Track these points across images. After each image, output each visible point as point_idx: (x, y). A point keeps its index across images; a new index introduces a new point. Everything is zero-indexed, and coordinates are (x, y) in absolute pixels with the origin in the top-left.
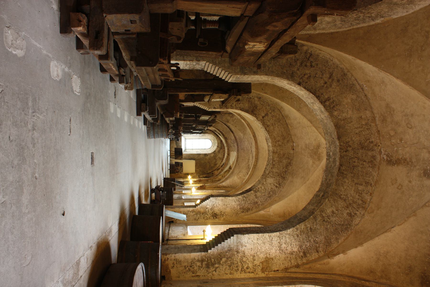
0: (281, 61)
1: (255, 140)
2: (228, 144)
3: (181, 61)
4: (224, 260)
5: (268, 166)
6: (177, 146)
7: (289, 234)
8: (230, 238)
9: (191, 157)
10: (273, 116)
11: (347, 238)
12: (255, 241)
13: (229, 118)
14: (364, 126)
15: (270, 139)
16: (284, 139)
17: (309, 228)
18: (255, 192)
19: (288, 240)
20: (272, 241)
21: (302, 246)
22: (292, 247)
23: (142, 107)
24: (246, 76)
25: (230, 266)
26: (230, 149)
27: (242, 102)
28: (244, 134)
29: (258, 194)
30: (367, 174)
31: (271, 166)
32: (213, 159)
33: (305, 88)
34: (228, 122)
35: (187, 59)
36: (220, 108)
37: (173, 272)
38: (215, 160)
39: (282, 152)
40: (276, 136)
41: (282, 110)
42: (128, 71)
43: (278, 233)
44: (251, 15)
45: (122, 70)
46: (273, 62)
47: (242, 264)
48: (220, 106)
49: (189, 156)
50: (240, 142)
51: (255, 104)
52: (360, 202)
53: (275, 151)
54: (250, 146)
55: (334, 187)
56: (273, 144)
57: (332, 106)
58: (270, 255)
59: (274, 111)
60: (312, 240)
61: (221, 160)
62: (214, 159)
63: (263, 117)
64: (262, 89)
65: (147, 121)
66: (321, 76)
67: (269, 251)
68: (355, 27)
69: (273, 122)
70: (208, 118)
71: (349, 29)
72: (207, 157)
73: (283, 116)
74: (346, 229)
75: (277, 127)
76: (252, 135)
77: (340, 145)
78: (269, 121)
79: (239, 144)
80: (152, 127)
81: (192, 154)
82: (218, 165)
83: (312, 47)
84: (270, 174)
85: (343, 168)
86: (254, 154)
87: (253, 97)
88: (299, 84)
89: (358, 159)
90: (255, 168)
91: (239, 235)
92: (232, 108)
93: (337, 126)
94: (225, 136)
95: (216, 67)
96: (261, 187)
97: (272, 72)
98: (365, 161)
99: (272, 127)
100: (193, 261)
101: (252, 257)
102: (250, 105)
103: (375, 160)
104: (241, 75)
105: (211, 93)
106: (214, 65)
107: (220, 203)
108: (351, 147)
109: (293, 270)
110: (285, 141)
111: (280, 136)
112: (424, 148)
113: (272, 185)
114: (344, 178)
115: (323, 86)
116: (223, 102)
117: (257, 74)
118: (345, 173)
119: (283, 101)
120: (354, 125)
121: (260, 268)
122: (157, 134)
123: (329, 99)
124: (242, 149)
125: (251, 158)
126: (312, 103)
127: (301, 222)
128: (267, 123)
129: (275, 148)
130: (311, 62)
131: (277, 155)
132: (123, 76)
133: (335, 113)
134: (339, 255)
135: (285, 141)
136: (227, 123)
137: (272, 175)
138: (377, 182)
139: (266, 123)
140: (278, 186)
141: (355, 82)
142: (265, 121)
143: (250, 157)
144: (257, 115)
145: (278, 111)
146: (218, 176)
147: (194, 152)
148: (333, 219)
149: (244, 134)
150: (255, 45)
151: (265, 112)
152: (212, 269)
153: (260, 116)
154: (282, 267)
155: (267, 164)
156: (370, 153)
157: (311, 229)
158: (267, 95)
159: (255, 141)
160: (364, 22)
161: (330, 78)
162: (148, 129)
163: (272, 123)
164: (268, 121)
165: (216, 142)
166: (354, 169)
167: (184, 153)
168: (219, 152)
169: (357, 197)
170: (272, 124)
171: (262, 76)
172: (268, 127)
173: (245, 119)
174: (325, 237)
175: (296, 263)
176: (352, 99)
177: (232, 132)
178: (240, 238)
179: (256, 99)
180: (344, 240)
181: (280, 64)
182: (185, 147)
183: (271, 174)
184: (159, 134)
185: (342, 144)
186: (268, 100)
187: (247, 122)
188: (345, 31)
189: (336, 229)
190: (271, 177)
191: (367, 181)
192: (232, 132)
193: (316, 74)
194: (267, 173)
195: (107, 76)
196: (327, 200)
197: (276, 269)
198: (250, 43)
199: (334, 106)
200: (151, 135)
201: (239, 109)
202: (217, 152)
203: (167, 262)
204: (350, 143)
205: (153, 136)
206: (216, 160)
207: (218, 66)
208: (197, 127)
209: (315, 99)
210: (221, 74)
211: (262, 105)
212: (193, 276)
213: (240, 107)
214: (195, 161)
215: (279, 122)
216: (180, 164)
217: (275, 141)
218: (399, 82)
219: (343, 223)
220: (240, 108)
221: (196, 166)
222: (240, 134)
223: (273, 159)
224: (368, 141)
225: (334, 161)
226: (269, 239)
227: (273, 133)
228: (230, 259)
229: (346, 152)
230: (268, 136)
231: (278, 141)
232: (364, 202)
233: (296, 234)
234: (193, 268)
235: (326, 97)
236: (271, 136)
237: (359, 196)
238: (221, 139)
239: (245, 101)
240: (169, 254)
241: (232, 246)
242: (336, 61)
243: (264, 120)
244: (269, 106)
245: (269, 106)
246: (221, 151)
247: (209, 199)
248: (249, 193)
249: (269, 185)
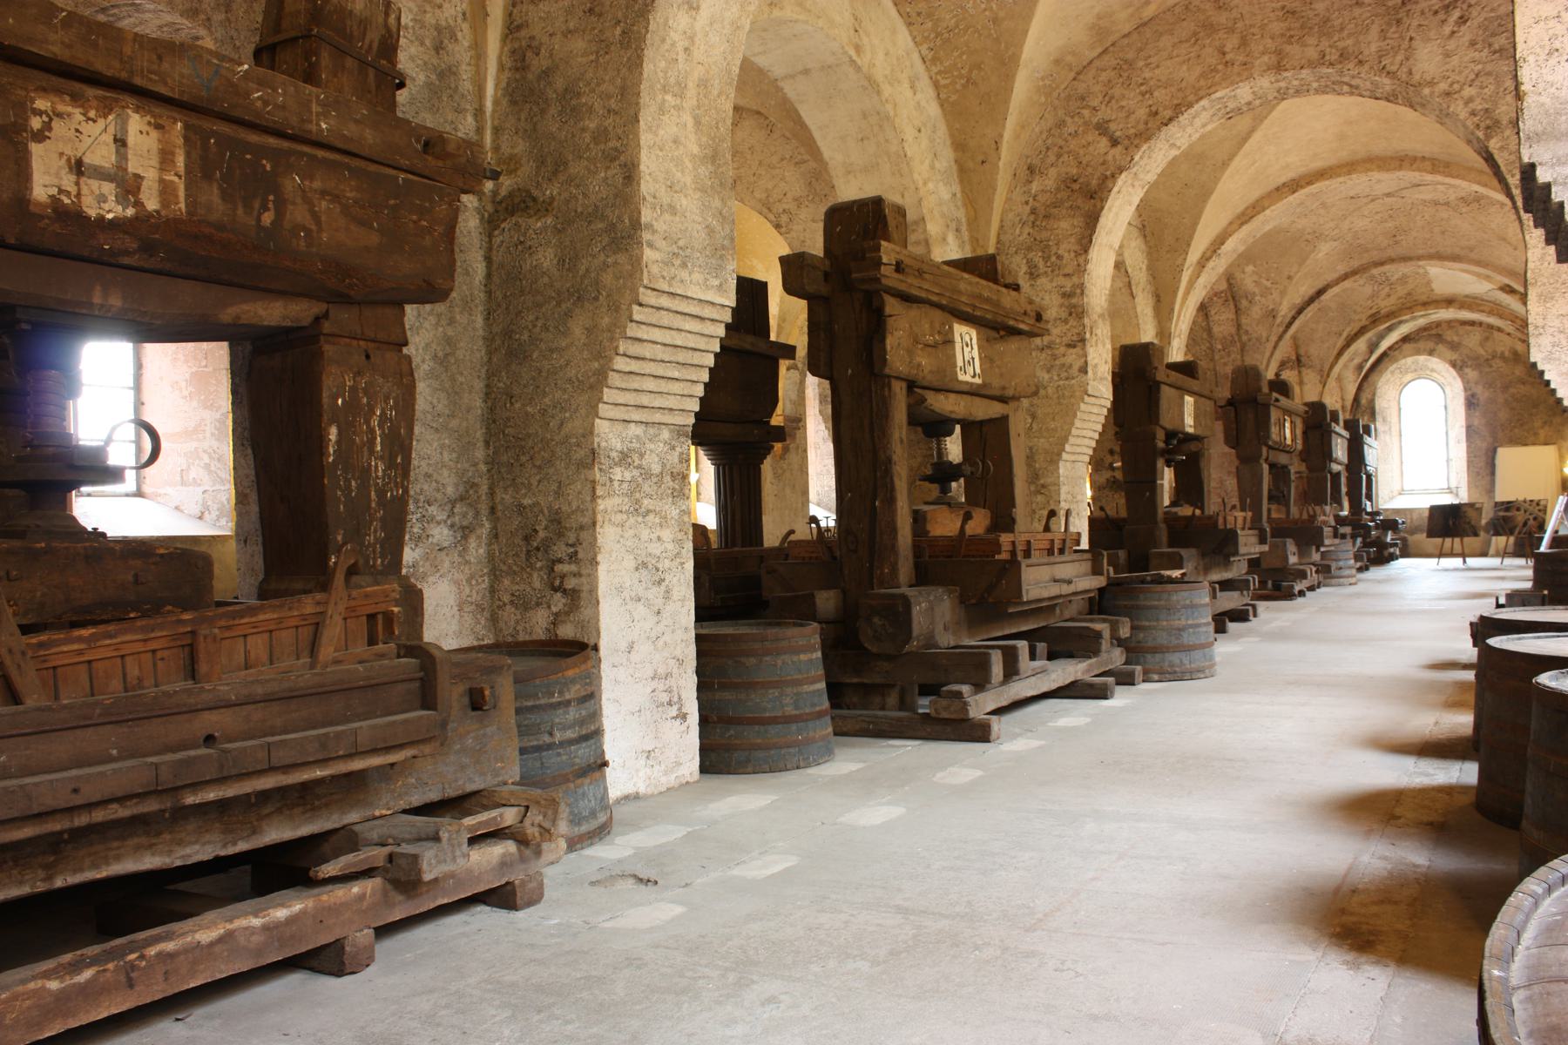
0: (579, 60)
1: (1309, 183)
2: (1401, 310)
3: (595, 539)
5: (1357, 87)
6: (1422, 531)
8: (1548, 186)
9: (1484, 466)
10: (1108, 99)
13: (1256, 312)
15: (1218, 95)
16: (1210, 28)
23: (945, 715)
26: (1424, 298)
27: (1054, 249)
28: (1318, 236)
31: (1351, 66)
32: (1488, 370)
34: (1272, 314)
35: (587, 510)
36: (1084, 345)
38: (1493, 363)
39: (1277, 27)
40: (1198, 70)
41: (1069, 58)
46: (584, 101)
48: (1075, 347)
49: (1478, 474)
50: (1366, 255)
51: (1058, 190)
53: (1274, 58)
54: (1366, 204)
56: (1239, 74)
59: (1083, 99)
61: (1496, 333)
62: (1491, 366)
63: (1115, 142)
64: (983, 162)
65: (1091, 686)
69: (1132, 95)
70: (1189, 400)
72: (1483, 394)
73: (1105, 51)
75: (1156, 71)
76: (1291, 198)
78: (1130, 113)
79: (1375, 256)
80: (1149, 656)
81: (1470, 463)
84: (1394, 68)
86: (1384, 181)
87: (1027, 203)
90: (1447, 165)
92: (1078, 291)
94: (1364, 323)
95: (614, 370)
97: (622, 95)
99: (1156, 94)
102: (1064, 211)
104: (640, 243)
105: (899, 389)
106: (606, 378)
110: (1222, 18)
111: (1197, 47)
117: (633, 164)
122: (1185, 635)
124: (1396, 242)
125: (1426, 194)
128: (1138, 122)
129: (1257, 63)
131: (1294, 50)
135: (1222, 18)
136: (1279, 320)
137: (1399, 58)
139: (1141, 127)
142: (1132, 131)
143: (1421, 196)
144: (1108, 173)
145: (1081, 77)
147: (1460, 452)
149: (1318, 236)
151: (1090, 139)
153: (1110, 157)
155: (1351, 94)
158: (1007, 135)
159: (1317, 180)
162: (1156, 677)
163: (1140, 98)
164: (1133, 116)
165: (1409, 360)
167: (1463, 497)
168: (1454, 347)
170: (1143, 94)
172: (1156, 113)
173: (1217, 237)
177: (1320, 293)
178: (1547, 113)
179: (1035, 187)
181: (592, 61)
182: (1442, 491)
183: (1392, 62)
184: (1183, 622)
186: (1037, 130)
187: (1235, 226)
190: (1407, 59)
192: (1320, 293)
194: (1387, 81)
200: (1186, 661)
201: (1083, 257)
202: (1455, 356)
205: (1197, 654)
206: (1494, 357)
207: (611, 360)
208: (1286, 445)
210: (679, 343)
211: (1059, 156)
213: (1073, 254)
214: (1501, 446)
215: (1130, 64)
216: (1502, 514)
217: (1220, 67)
220: (1077, 254)
221: (1526, 445)
222: (1325, 259)
223: (1312, 65)
227: (1183, 85)
230: (1204, 109)
231: (1224, 54)
236: (1202, 93)
238: (1397, 343)
239: (1045, 235)
243: (1128, 137)
244: (1061, 124)
246: (1449, 339)
247: (1540, 367)
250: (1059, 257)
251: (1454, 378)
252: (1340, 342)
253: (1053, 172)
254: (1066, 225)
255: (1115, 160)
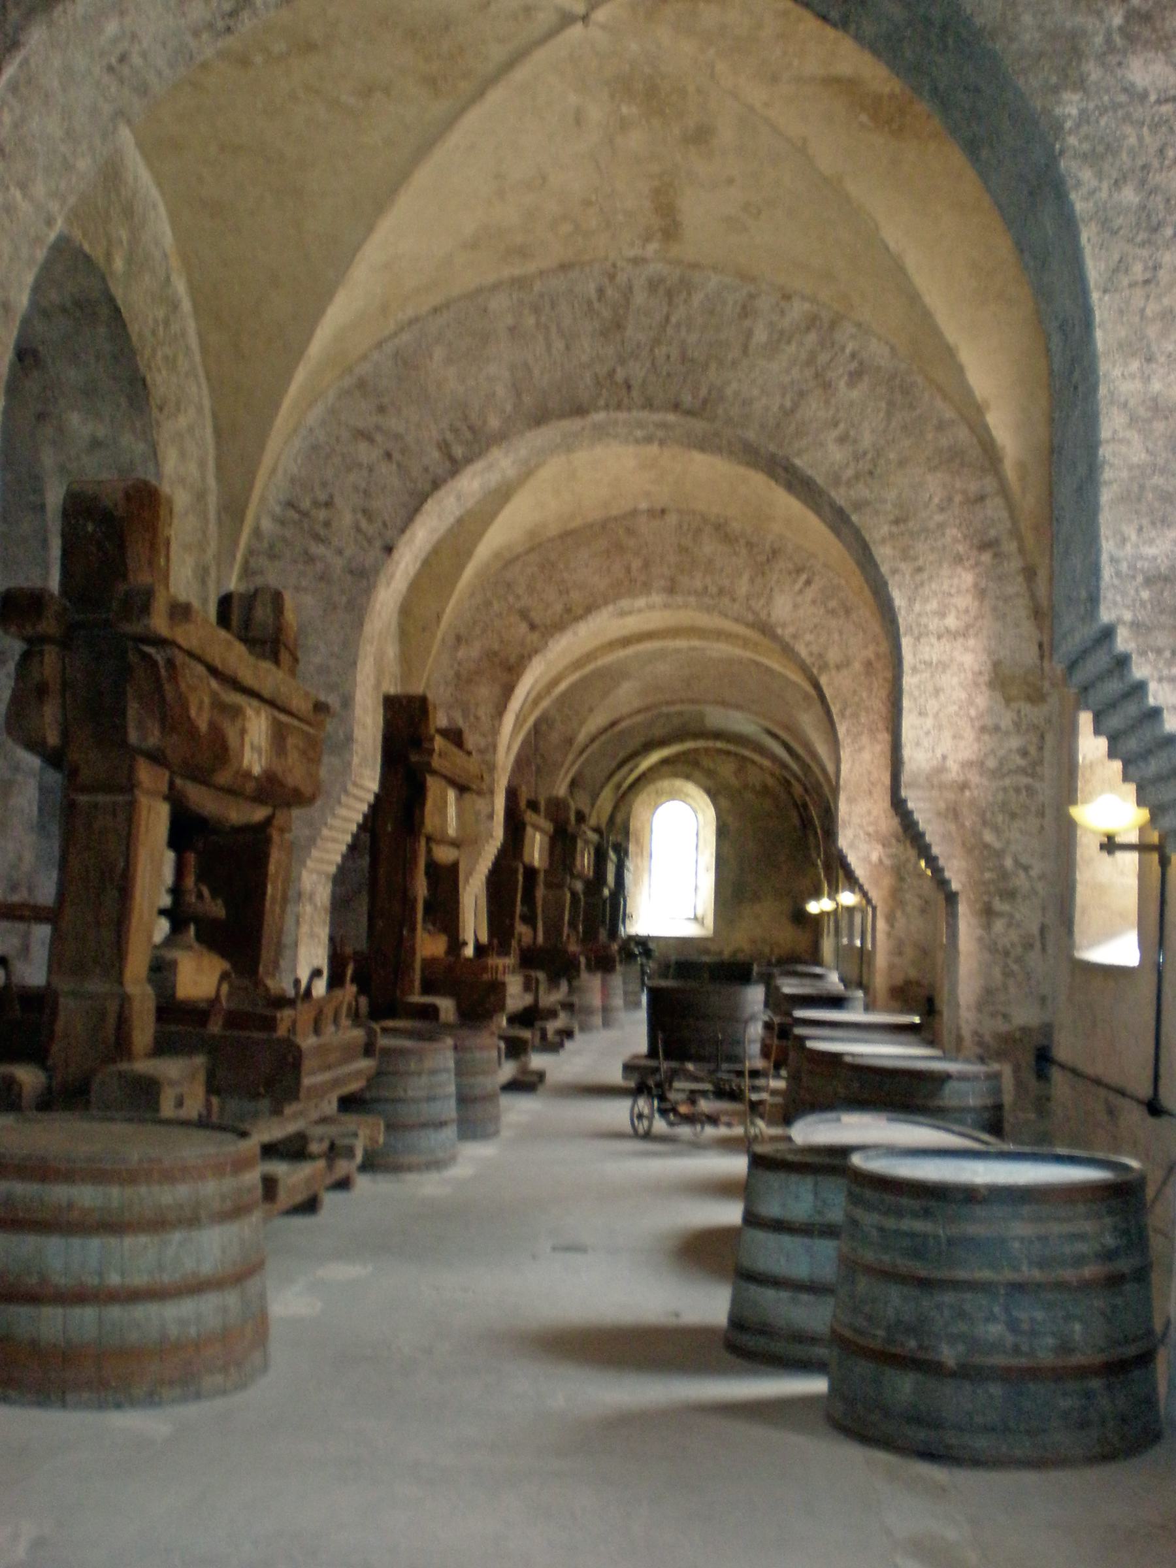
4: (989, 837)
7: (911, 601)
11: (940, 389)
12: (929, 722)
14: (543, 319)
16: (620, 548)
17: (894, 529)
18: (824, 667)
19: (933, 605)
20: (932, 663)
21: (958, 553)
22: (959, 592)
24: (358, 734)
25: (1013, 816)
29: (833, 656)
30: (712, 312)
33: (403, 531)
37: (1025, 1016)
42: (319, 1130)
43: (906, 642)
44: (167, 774)
45: (315, 1147)
47: (1010, 771)
52: (812, 338)
55: (751, 435)
57: (468, 435)
58: (980, 673)
60: (939, 518)
66: (365, 473)
67: (970, 675)
68: (198, 358)
71: (203, 380)
74: (906, 391)
77: (607, 407)
82: (770, 782)
83: (263, 499)
85: (687, 399)
88: (389, 550)
89: (657, 341)
91: (905, 778)
93: (540, 418)
96: (808, 644)
98: (667, 319)
100: (991, 947)
101: (986, 737)
103: (662, 280)
105: (423, 842)
107: (861, 808)
108: (614, 370)
109: (1042, 589)
110: (631, 543)
112: (611, 141)
113: (799, 599)
114: (722, 398)
115: (399, 465)
116: (462, 789)
118: (703, 392)
119: (469, 554)
120: (538, 354)
121: (1026, 708)
123: (444, 447)
126: (459, 498)
127: (871, 554)
130: (316, 504)
132: (332, 1146)
133: (494, 423)
134: (991, 426)
135: (631, 543)
137: (762, 602)
138: (745, 277)
140: (804, 577)
141: (389, 348)
146: (807, 783)
148: (867, 440)
150: (252, 744)
152: (1020, 881)
154: (1028, 627)
156: (640, 298)
157: (897, 522)
158: (448, 610)
160: (184, 334)
161: (371, 440)
166: (692, 360)
168: (710, 773)
169: (792, 348)
171: (359, 678)
174: (929, 470)
175: (1020, 579)
176: (449, 361)
179: (460, 654)
180: (945, 397)
183: (758, 605)
185: (602, 402)
188: (212, 390)
189: (904, 428)
191: (738, 309)
193: (356, 488)
195: (330, 1200)
196: (798, 462)
197: (1035, 650)
198: (246, 763)
199: (471, 428)
202: (709, 783)
203: (988, 1038)
204: (602, 370)
209: (441, 493)
212: (1044, 949)
218: (386, 226)
219: (883, 405)
220: (492, 717)
224: (596, 305)
225: (663, 425)
226: (924, 675)
228: (988, 815)
229: (629, 387)
232: (812, 322)
233: (912, 576)
234: (1013, 945)
235: (436, 454)
237: (789, 342)
240: (958, 1028)
241: (942, 805)
242: (314, 416)
244: (488, 604)
245: (488, 604)
248: (828, 695)
249: (801, 612)
250: (477, 718)
251: (708, 806)
252: (614, 765)
253: (477, 645)
254: (485, 691)
255: (532, 642)
